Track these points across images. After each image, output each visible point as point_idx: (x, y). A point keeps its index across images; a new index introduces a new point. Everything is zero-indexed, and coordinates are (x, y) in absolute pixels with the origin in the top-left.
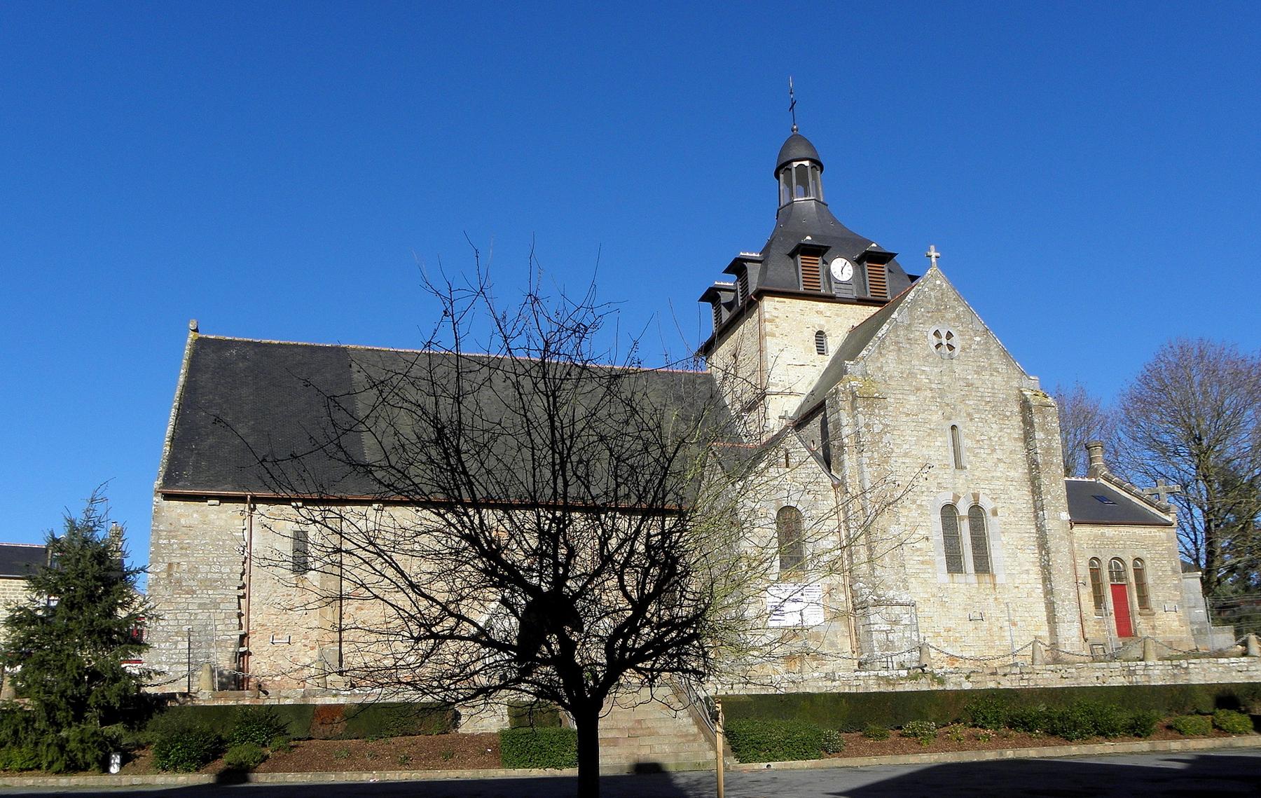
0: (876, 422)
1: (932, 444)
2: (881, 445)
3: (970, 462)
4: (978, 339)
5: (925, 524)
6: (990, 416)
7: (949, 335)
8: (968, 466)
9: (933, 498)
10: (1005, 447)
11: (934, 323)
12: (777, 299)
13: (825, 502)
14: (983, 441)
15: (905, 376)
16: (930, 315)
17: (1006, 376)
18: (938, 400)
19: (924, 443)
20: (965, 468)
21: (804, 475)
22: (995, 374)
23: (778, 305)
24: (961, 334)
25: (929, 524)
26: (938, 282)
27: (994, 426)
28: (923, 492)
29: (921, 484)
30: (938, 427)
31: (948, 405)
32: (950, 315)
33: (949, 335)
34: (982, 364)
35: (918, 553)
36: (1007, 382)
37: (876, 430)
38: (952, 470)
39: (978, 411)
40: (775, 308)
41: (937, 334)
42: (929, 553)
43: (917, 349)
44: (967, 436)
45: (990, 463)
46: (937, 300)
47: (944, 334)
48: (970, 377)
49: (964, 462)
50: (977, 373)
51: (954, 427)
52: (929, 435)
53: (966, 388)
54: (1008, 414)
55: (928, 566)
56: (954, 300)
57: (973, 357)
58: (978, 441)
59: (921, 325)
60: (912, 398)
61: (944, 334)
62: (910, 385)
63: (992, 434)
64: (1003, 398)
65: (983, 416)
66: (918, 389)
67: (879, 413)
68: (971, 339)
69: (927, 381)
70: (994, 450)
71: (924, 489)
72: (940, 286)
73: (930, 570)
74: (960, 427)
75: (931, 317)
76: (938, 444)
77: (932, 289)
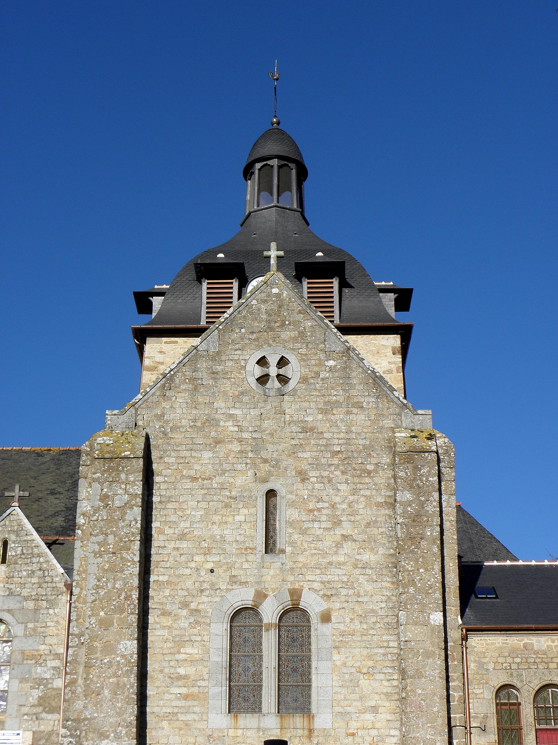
0: (120, 492)
1: (230, 519)
2: (121, 524)
3: (292, 544)
4: (331, 363)
5: (199, 638)
6: (338, 473)
7: (283, 362)
8: (289, 549)
9: (217, 599)
10: (358, 518)
11: (260, 347)
12: (165, 339)
13: (51, 611)
14: (319, 510)
15: (199, 424)
16: (254, 336)
17: (373, 413)
18: (250, 455)
19: (216, 518)
20: (283, 551)
21: (25, 573)
22: (355, 410)
23: (165, 347)
24: (303, 359)
25: (206, 638)
26: (275, 291)
27: (343, 487)
28: (202, 591)
29: (202, 579)
30: (245, 494)
31: (265, 461)
32: (286, 335)
33: (283, 362)
34: (335, 398)
35: (180, 683)
36: (373, 422)
37: (117, 503)
38: (259, 556)
39: (317, 466)
40: (161, 352)
41: (262, 362)
42: (199, 683)
43: (226, 386)
44: (292, 504)
45: (328, 543)
46: (270, 315)
47: (273, 360)
48: (310, 419)
49: (281, 542)
50: (324, 412)
51: (271, 494)
52: (227, 506)
53: (301, 436)
54: (370, 467)
55: (195, 703)
56: (300, 312)
57: (319, 390)
58: (311, 511)
59: (239, 352)
60: (207, 455)
61: (273, 360)
62: (206, 437)
63: (338, 499)
64: (364, 446)
65: (325, 474)
66: (218, 442)
67: (127, 478)
68: (321, 364)
69: (236, 429)
70: (338, 523)
71: (206, 586)
72: (278, 295)
73: (197, 709)
74: (282, 491)
75: (257, 339)
76: (238, 518)
77: (265, 302)
